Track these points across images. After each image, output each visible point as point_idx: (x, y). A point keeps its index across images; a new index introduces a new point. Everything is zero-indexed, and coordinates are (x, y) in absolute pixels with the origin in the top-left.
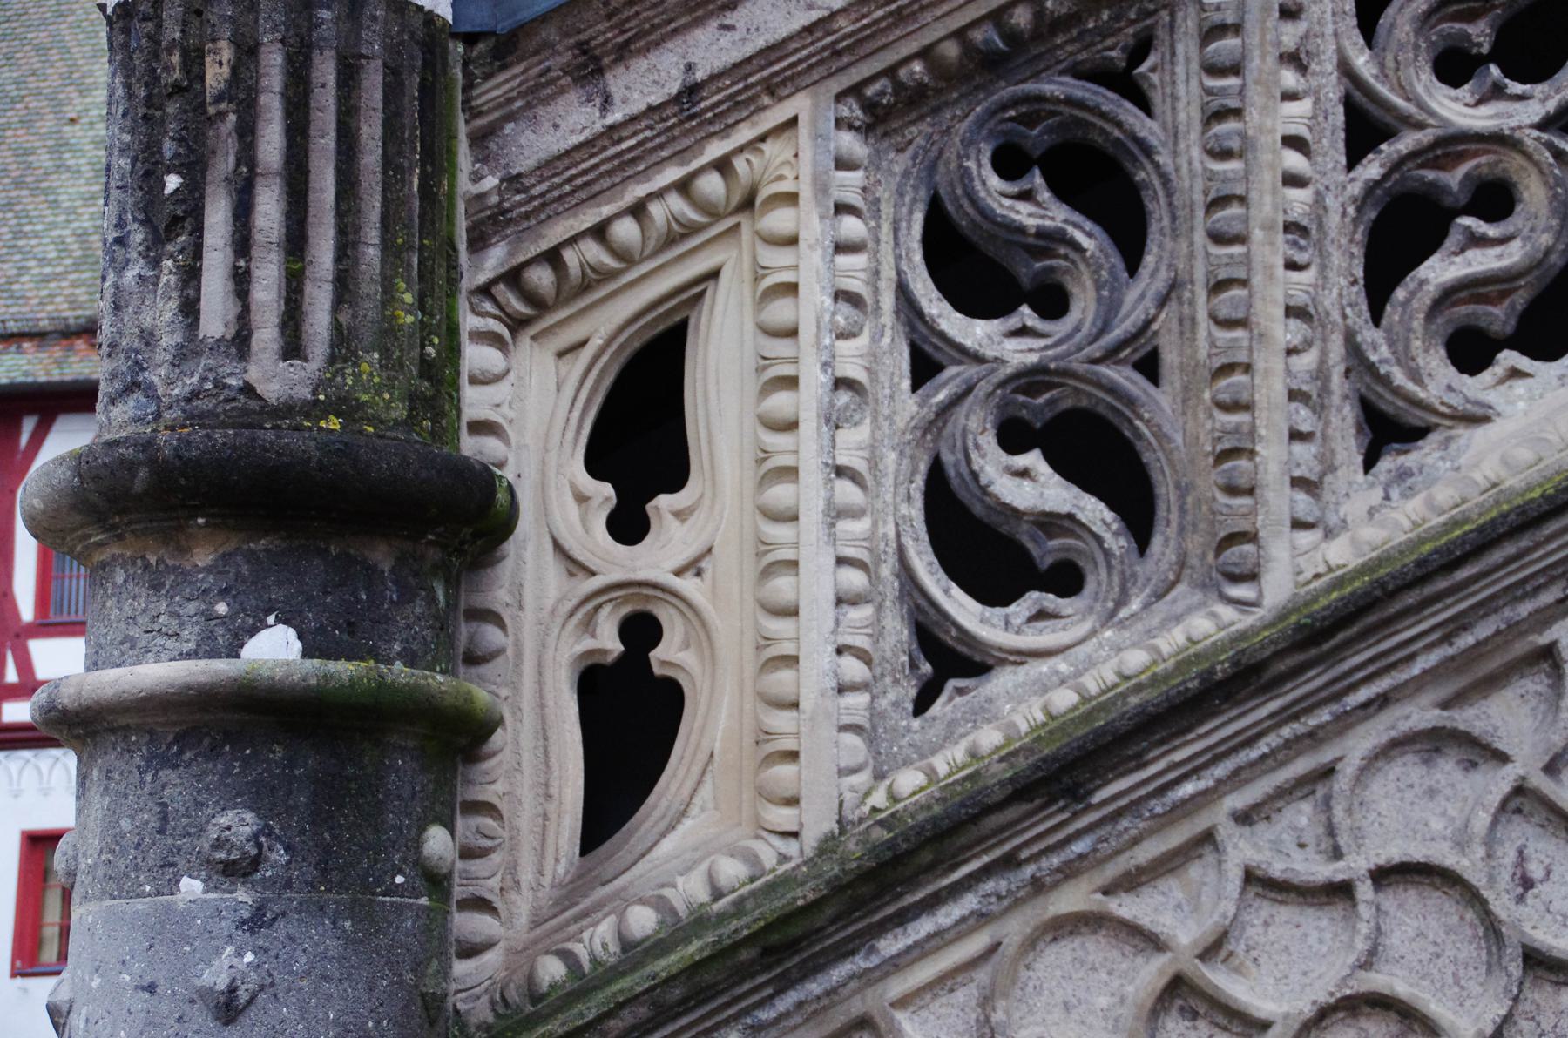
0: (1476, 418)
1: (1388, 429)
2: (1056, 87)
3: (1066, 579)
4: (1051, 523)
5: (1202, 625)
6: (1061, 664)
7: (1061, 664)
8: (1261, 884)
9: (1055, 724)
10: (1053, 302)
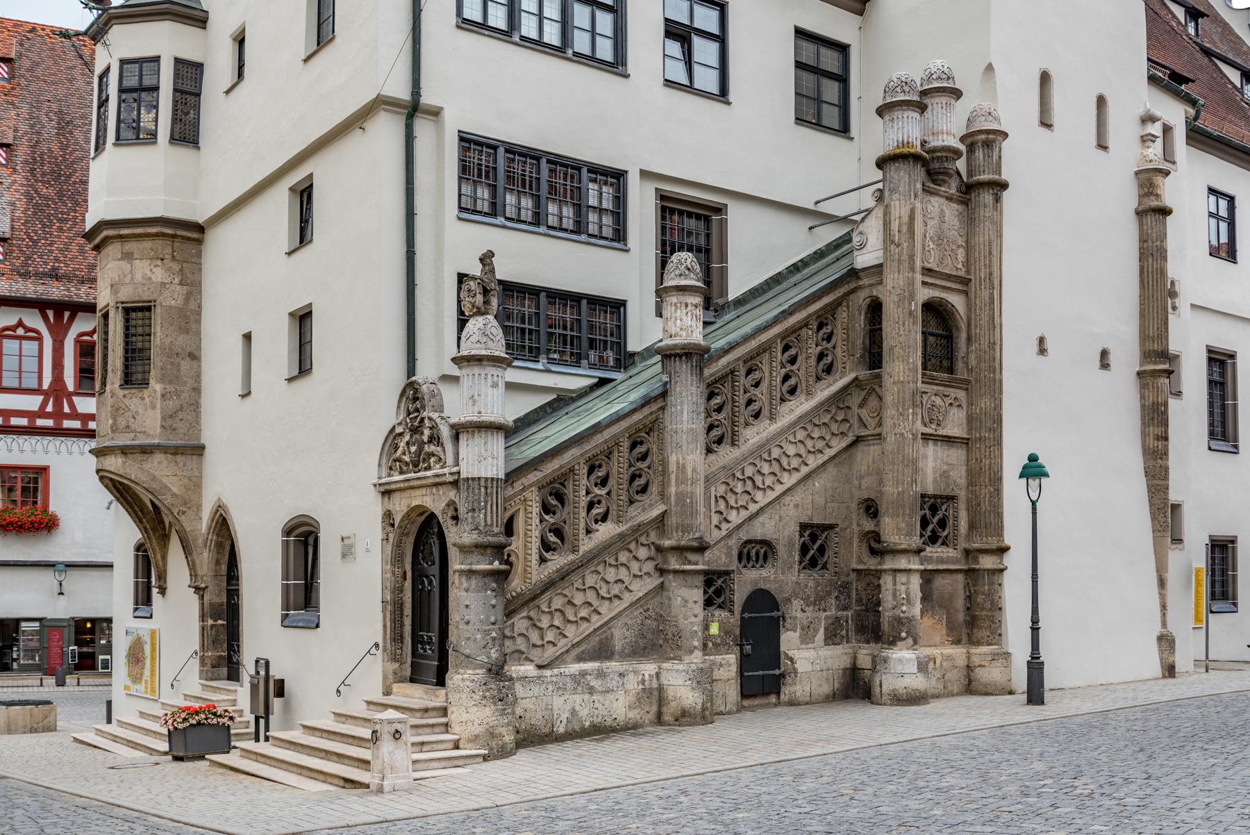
1: (588, 532)
3: (554, 550)
5: (571, 557)
6: (558, 561)
7: (558, 561)
9: (558, 571)
10: (554, 513)
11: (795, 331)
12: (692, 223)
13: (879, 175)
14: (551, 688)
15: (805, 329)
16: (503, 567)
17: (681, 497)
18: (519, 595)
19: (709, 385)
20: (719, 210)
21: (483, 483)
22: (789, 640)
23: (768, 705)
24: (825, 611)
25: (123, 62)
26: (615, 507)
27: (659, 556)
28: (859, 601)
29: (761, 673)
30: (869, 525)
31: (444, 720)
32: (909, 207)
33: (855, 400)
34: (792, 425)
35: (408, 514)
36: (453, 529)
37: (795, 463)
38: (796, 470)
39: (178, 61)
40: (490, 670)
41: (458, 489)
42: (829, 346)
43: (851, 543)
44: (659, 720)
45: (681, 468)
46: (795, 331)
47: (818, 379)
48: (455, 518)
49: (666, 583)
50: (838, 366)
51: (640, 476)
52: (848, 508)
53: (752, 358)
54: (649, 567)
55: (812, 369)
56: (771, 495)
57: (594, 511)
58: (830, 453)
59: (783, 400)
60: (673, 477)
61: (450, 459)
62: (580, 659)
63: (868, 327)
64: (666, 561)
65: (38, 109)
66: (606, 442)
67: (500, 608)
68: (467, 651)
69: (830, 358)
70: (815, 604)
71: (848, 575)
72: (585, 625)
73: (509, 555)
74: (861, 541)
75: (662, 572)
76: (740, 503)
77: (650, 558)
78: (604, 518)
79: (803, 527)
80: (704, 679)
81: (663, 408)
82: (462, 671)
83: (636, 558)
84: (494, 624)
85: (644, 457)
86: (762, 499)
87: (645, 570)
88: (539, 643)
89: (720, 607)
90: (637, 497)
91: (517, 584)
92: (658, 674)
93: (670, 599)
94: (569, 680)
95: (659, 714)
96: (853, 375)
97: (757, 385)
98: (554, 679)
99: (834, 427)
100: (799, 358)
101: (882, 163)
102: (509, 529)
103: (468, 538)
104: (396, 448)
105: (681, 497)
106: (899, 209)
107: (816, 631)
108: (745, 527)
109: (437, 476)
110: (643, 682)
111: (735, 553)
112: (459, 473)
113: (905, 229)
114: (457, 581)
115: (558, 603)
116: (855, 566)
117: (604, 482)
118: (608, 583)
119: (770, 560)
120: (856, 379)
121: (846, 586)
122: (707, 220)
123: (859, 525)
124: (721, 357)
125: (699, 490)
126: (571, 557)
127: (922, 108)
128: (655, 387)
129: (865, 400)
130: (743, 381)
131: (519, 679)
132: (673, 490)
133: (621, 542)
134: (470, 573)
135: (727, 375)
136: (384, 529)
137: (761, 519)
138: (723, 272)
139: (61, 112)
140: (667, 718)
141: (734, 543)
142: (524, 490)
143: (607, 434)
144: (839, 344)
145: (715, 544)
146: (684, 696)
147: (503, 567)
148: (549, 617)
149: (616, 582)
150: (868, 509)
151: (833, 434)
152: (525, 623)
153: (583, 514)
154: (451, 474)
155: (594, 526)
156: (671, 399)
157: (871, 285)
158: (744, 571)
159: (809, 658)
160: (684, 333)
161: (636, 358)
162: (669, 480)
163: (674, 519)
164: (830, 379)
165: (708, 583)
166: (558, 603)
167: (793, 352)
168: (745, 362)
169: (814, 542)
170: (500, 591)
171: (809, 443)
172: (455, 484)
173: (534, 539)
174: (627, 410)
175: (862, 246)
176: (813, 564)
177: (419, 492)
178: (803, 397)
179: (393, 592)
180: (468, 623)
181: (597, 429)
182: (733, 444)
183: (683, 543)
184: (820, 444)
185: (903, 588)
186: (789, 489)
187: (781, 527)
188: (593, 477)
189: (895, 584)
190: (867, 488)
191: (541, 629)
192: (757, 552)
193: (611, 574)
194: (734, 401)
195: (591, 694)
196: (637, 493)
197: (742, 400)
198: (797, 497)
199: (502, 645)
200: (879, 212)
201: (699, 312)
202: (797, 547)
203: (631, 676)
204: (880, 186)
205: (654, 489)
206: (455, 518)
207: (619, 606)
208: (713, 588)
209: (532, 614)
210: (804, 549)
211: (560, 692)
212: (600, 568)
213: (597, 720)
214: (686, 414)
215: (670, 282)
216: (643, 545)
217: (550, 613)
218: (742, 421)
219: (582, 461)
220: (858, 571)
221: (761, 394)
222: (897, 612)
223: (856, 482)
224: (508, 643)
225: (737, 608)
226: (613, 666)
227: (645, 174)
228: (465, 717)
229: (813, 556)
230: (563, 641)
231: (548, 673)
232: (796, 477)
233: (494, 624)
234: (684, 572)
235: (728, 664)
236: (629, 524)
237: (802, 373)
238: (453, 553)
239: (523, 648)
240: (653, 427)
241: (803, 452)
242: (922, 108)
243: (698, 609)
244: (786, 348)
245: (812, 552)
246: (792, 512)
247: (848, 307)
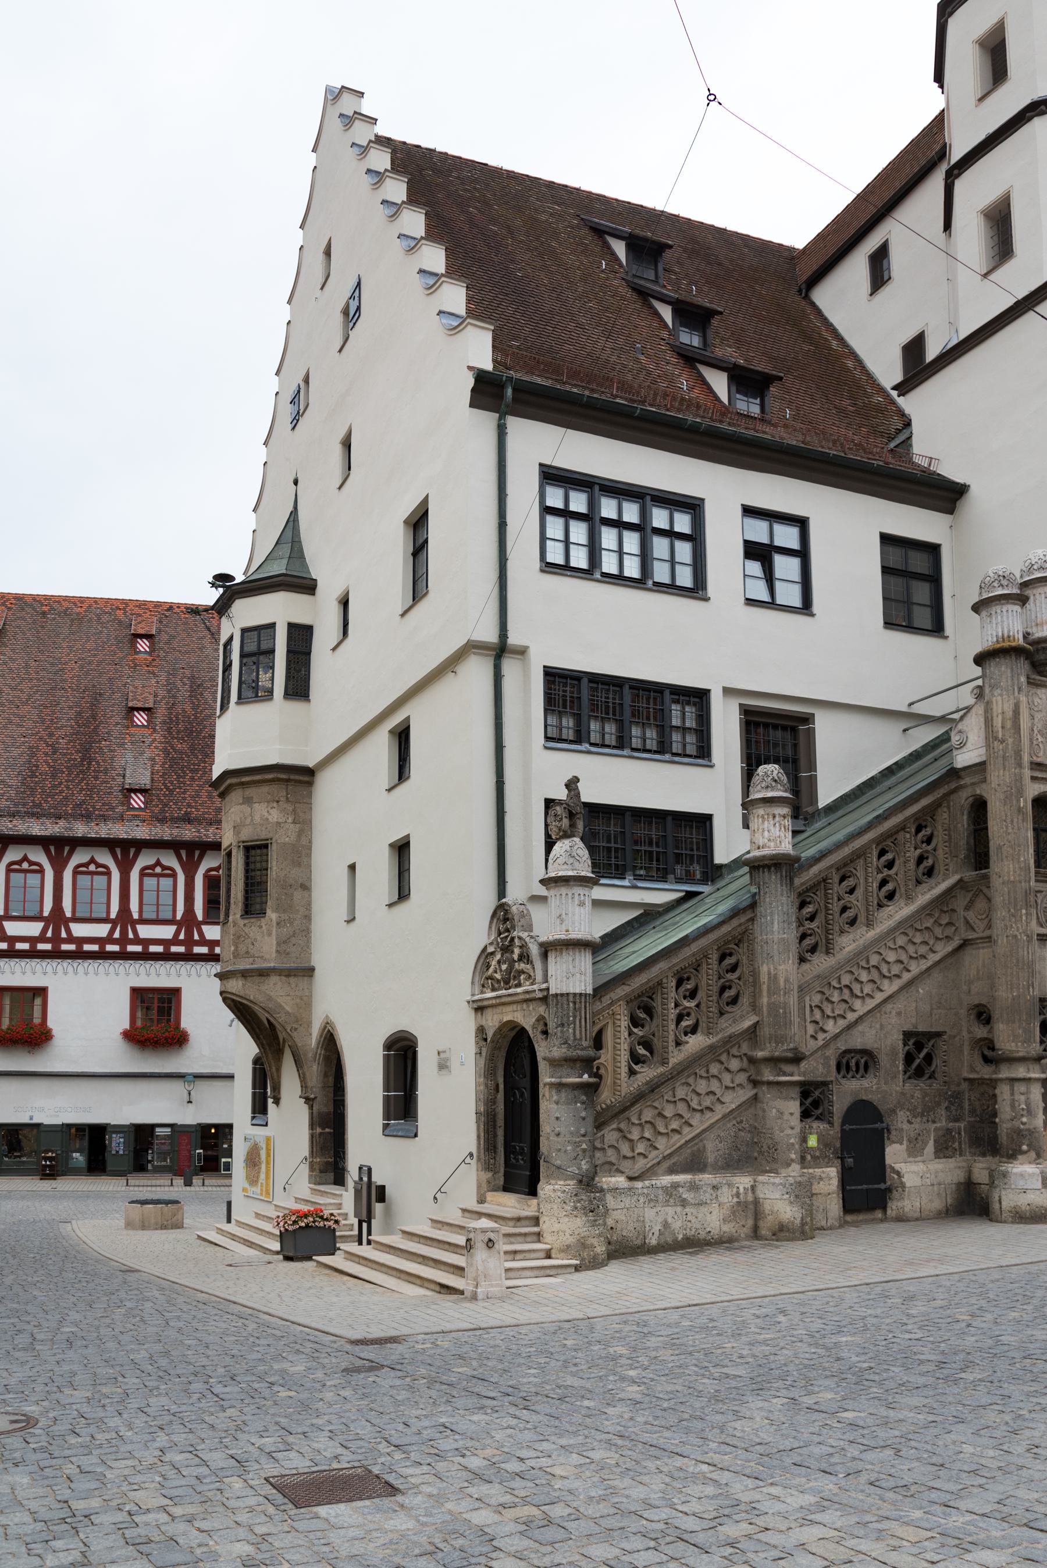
0: (687, 1043)
1: (678, 1044)
2: (645, 999)
3: (644, 1062)
4: (644, 1055)
5: (661, 1069)
6: (647, 1073)
7: (647, 1073)
8: (667, 1101)
10: (643, 1026)
11: (891, 835)
12: (778, 735)
13: (978, 671)
14: (642, 1200)
15: (902, 833)
16: (592, 1080)
17: (773, 1007)
18: (608, 1107)
19: (800, 894)
20: (807, 719)
21: (571, 998)
22: (894, 1154)
23: (874, 1221)
24: (934, 1122)
25: (244, 631)
26: (704, 1019)
27: (752, 1067)
28: (973, 1111)
29: (865, 1187)
30: (981, 1032)
31: (536, 1229)
32: (1012, 702)
33: (961, 901)
34: (892, 931)
35: (500, 1029)
36: (543, 1044)
37: (896, 969)
38: (898, 976)
39: (291, 626)
40: (580, 1182)
41: (547, 1005)
42: (929, 848)
43: (962, 1051)
44: (755, 1234)
45: (773, 978)
46: (891, 835)
47: (919, 882)
48: (545, 1033)
49: (760, 1095)
50: (940, 868)
51: (730, 987)
52: (956, 1014)
53: (845, 865)
54: (741, 1078)
55: (912, 873)
56: (871, 1004)
57: (686, 1023)
58: (937, 957)
59: (880, 906)
60: (765, 987)
61: (539, 976)
62: (671, 1171)
63: (972, 827)
64: (759, 1072)
65: (174, 675)
66: (694, 955)
67: (590, 1120)
68: (558, 1163)
69: (930, 861)
70: (922, 1115)
71: (959, 1085)
72: (677, 1137)
73: (598, 1068)
74: (972, 1049)
75: (755, 1083)
76: (837, 1012)
77: (742, 1070)
78: (694, 1030)
79: (907, 1035)
80: (803, 1193)
81: (752, 919)
82: (553, 1182)
83: (728, 1070)
84: (584, 1136)
85: (733, 968)
86: (861, 1008)
87: (738, 1081)
88: (629, 1154)
89: (818, 1118)
90: (728, 1009)
91: (606, 1097)
92: (753, 1188)
93: (764, 1111)
94: (660, 1192)
95: (756, 1229)
96: (957, 877)
97: (852, 891)
98: (645, 1191)
99: (938, 932)
100: (897, 863)
101: (980, 659)
102: (598, 1042)
103: (558, 1052)
104: (488, 967)
105: (773, 1007)
106: (1002, 705)
107: (925, 1144)
108: (843, 1037)
109: (527, 992)
110: (738, 1195)
111: (833, 1063)
112: (548, 989)
113: (1009, 724)
114: (547, 1094)
115: (648, 1115)
116: (966, 1075)
117: (693, 994)
118: (699, 1094)
119: (871, 1070)
120: (961, 880)
121: (957, 1096)
122: (794, 730)
123: (969, 1032)
124: (812, 866)
125: (793, 1000)
126: (661, 1069)
127: (1022, 600)
128: (745, 899)
129: (971, 902)
130: (837, 889)
131: (610, 1190)
132: (765, 1000)
133: (712, 1053)
134: (560, 1086)
135: (819, 883)
136: (477, 1043)
137: (860, 1028)
138: (813, 781)
139: (193, 677)
140: (764, 1232)
141: (832, 1053)
142: (612, 1004)
143: (695, 947)
144: (940, 845)
145: (811, 1055)
146: (782, 1210)
147: (592, 1080)
148: (639, 1128)
149: (708, 1094)
150: (979, 1015)
151: (937, 939)
152: (616, 1135)
153: (672, 1026)
154: (541, 990)
155: (684, 1038)
156: (760, 910)
157: (973, 784)
158: (843, 1081)
159: (918, 1172)
160: (772, 844)
161: (724, 870)
162: (761, 991)
164: (932, 881)
165: (805, 1095)
166: (648, 1115)
167: (889, 856)
168: (838, 869)
169: (919, 1051)
170: (590, 1103)
171: (911, 949)
172: (545, 1000)
173: (623, 1052)
174: (715, 922)
175: (962, 745)
176: (919, 1073)
177: (510, 1008)
178: (902, 902)
179: (486, 1104)
180: (558, 1135)
181: (684, 942)
182: (827, 953)
183: (777, 1054)
184: (923, 950)
186: (890, 997)
187: (883, 1036)
188: (682, 989)
191: (631, 1141)
192: (857, 1062)
193: (702, 1086)
194: (827, 909)
195: (684, 1206)
196: (728, 1004)
197: (836, 907)
198: (899, 1004)
199: (592, 1157)
200: (979, 709)
201: (788, 822)
202: (901, 1056)
203: (725, 1189)
204: (980, 682)
205: (745, 1000)
206: (545, 1033)
207: (711, 1118)
208: (810, 1100)
209: (622, 1126)
210: (909, 1059)
211: (652, 1204)
212: (691, 1080)
213: (689, 1233)
214: (777, 924)
215: (756, 795)
216: (734, 1056)
217: (640, 1125)
218: (837, 928)
219: (670, 974)
220: (970, 1081)
221: (856, 900)
223: (965, 988)
224: (598, 1154)
225: (837, 1120)
226: (706, 1178)
227: (728, 691)
228: (557, 1227)
229: (919, 1065)
230: (654, 1153)
231: (639, 1184)
232: (896, 985)
233: (584, 1136)
234: (778, 1083)
235: (828, 1178)
236: (720, 1036)
237: (900, 878)
238: (543, 1067)
239: (613, 1159)
240: (742, 938)
241: (904, 957)
242: (1022, 600)
243: (795, 1121)
244: (882, 853)
245: (917, 1061)
246: (894, 1020)
247: (949, 808)
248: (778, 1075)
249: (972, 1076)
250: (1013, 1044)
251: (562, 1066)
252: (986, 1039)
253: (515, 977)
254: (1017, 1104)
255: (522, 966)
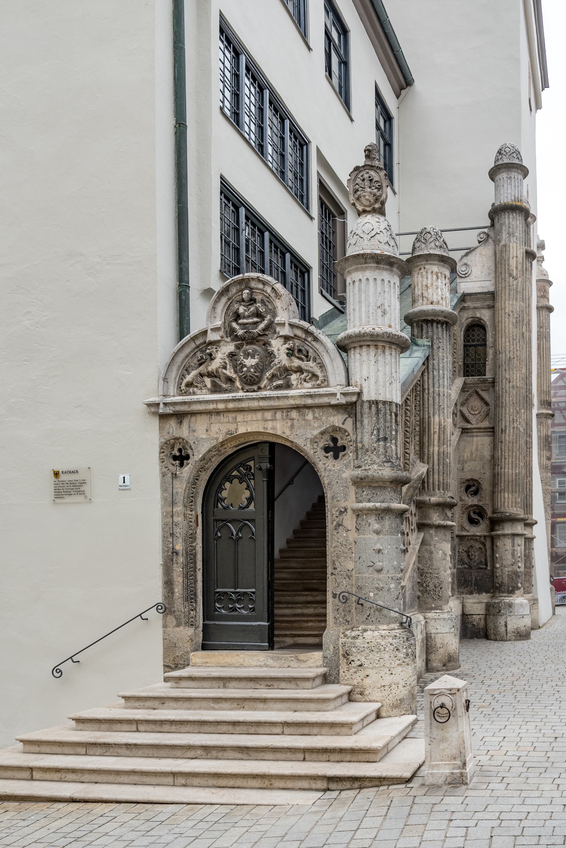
30: (472, 501)
150: (467, 488)
163: (436, 476)
177: (249, 416)
180: (379, 571)
185: (519, 548)
189: (513, 546)
190: (470, 471)
222: (515, 567)
248: (444, 520)
249: (465, 533)
250: (515, 509)
251: (385, 488)
252: (475, 505)
253: (273, 376)
254: (516, 552)
255: (296, 363)
